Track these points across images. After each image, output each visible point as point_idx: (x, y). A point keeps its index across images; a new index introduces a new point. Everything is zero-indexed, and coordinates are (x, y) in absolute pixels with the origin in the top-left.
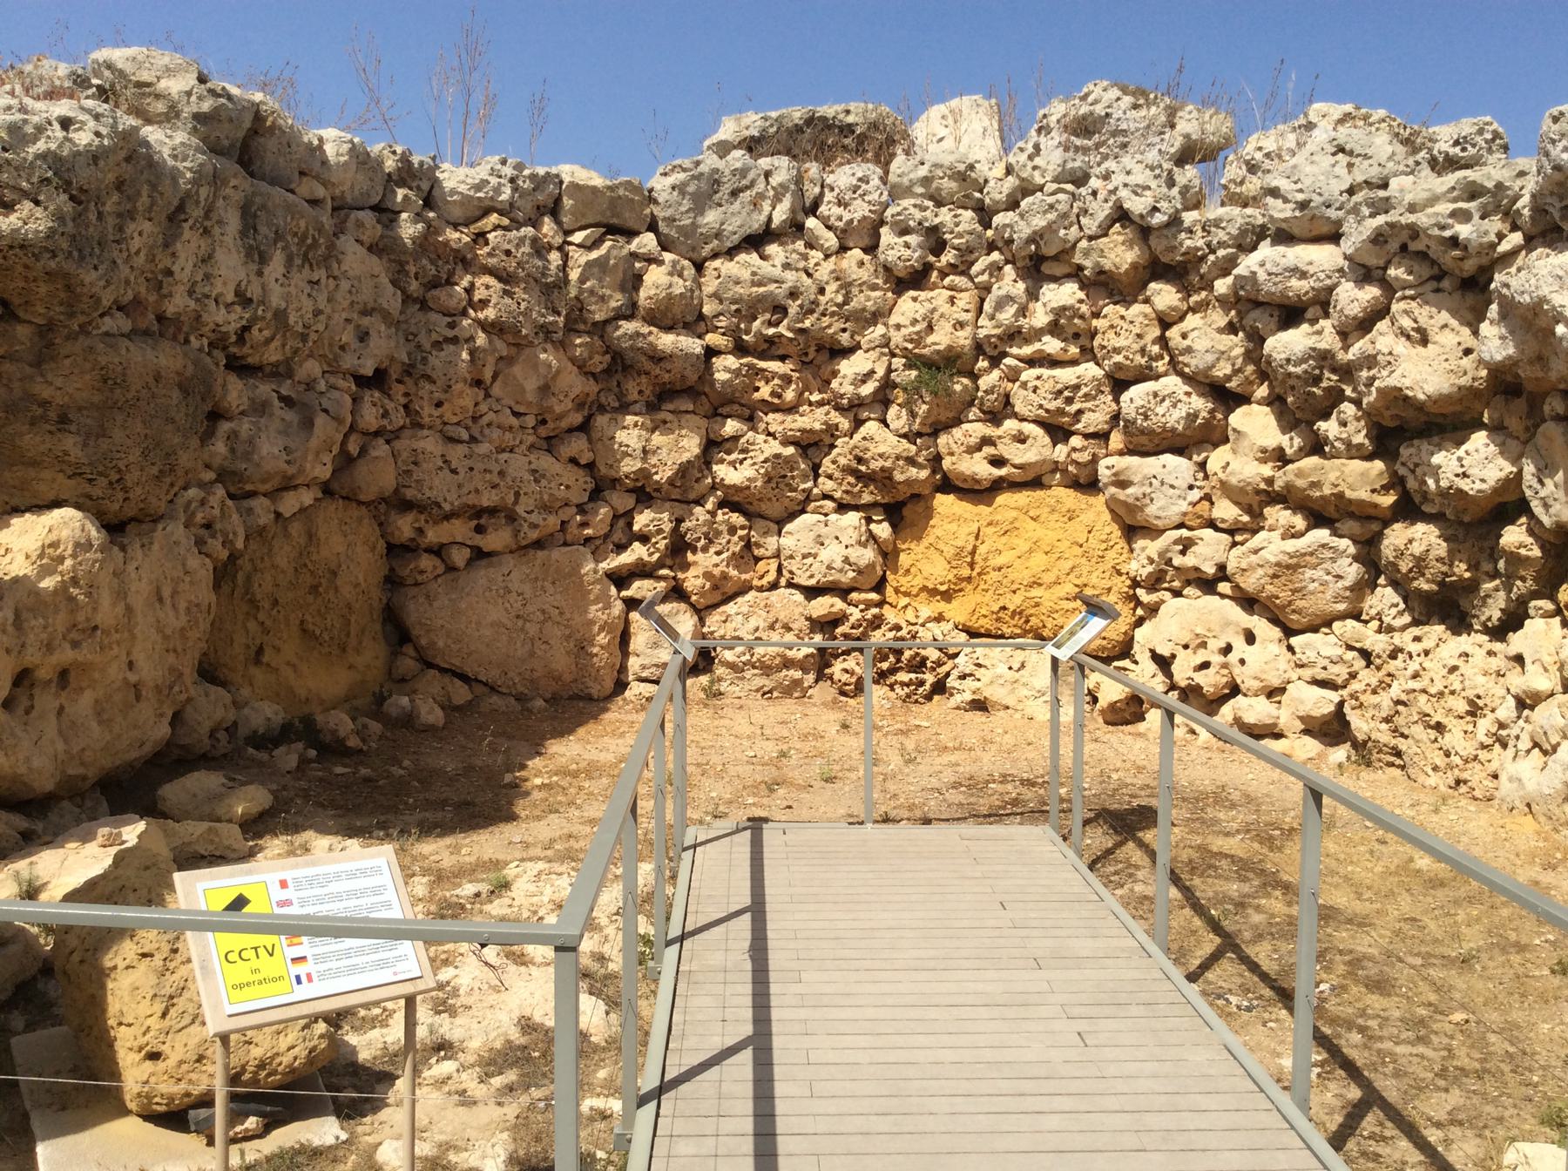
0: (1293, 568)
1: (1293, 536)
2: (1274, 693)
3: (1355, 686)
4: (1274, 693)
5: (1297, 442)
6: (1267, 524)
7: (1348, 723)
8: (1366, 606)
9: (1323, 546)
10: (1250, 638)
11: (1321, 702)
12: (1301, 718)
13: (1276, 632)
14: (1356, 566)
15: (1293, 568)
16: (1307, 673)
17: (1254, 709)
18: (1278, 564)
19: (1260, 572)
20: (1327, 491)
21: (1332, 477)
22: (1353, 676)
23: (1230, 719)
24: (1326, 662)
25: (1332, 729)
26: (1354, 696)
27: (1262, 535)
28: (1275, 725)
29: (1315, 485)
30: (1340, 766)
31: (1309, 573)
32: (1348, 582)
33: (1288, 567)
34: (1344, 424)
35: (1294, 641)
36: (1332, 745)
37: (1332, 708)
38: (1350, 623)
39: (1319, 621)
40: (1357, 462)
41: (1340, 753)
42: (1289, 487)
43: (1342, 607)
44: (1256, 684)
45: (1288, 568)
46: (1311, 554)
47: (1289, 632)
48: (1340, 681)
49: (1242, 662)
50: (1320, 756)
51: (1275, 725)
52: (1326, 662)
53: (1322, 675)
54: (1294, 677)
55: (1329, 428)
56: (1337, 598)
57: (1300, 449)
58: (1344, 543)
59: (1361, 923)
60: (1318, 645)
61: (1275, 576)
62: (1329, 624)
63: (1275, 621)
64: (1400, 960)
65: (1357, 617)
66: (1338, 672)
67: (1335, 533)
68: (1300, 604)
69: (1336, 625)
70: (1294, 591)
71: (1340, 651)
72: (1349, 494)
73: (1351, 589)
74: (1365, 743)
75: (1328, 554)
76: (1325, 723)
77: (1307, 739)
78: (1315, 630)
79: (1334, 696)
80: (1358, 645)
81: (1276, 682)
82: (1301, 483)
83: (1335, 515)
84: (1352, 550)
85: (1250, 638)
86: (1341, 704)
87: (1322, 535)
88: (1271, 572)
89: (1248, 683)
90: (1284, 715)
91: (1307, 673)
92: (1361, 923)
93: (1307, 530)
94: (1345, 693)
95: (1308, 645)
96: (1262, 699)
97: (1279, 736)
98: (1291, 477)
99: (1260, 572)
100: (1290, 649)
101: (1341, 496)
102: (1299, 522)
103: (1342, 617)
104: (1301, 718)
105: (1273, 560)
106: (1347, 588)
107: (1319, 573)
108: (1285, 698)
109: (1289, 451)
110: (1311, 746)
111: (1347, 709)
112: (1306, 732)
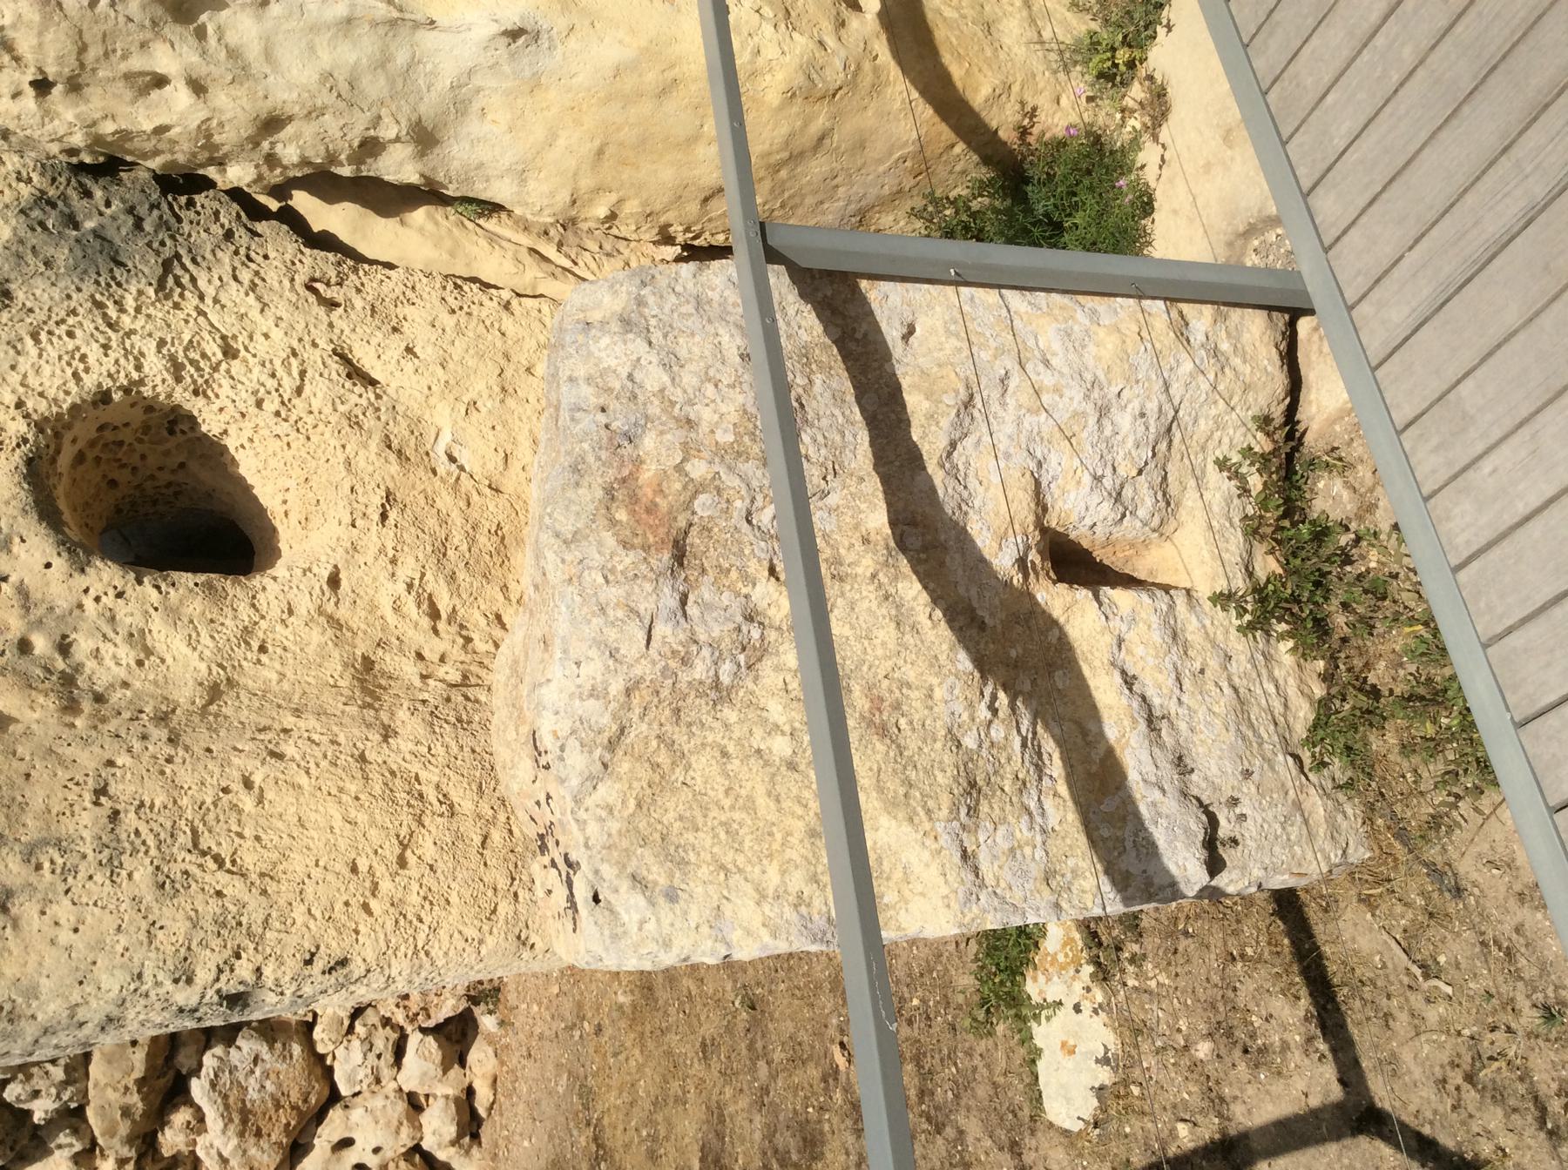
0: (245, 1114)
1: (200, 1117)
2: (415, 1104)
3: (400, 1017)
4: (415, 1104)
5: (63, 1138)
6: (185, 1150)
7: (448, 1021)
8: (294, 1019)
9: (213, 1085)
10: (347, 1143)
11: (422, 1056)
12: (445, 1072)
13: (335, 1114)
14: (240, 1042)
15: (245, 1114)
16: (386, 1073)
17: (438, 1129)
18: (241, 1134)
19: (253, 1151)
20: (135, 1099)
21: (112, 1095)
22: (386, 1022)
23: (452, 1150)
24: (371, 1057)
25: (456, 1036)
26: (413, 1019)
27: (200, 1153)
28: (457, 1101)
29: (126, 1112)
30: (502, 1023)
31: (253, 1094)
32: (263, 1049)
33: (244, 1121)
34: (36, 1094)
35: (344, 1090)
36: (477, 1027)
37: (430, 1039)
38: (318, 1034)
39: (319, 1071)
40: (92, 1068)
41: (487, 1022)
42: (130, 1141)
43: (296, 1049)
44: (405, 1131)
45: (245, 1120)
46: (225, 1097)
47: (334, 1097)
48: (396, 1036)
49: (376, 1150)
50: (491, 1040)
51: (457, 1101)
52: (371, 1057)
53: (389, 1057)
54: (393, 1085)
55: (40, 1110)
56: (286, 1056)
57: (75, 1132)
58: (209, 1061)
59: (717, 1117)
60: (348, 1067)
61: (258, 1134)
62: (322, 1057)
63: (320, 1116)
64: (765, 1090)
65: (310, 1026)
66: (383, 1040)
67: (196, 1071)
68: (295, 1096)
69: (320, 1049)
70: (278, 1106)
71: (356, 1043)
72: (138, 1073)
73: (271, 1042)
74: (470, 998)
75: (225, 1078)
76: (449, 1038)
77: (473, 1056)
78: (330, 1070)
79: (414, 1039)
80: (347, 1023)
81: (402, 1106)
82: (124, 1128)
83: (171, 1074)
84: (218, 1050)
85: (347, 1143)
86: (424, 1031)
87: (198, 1089)
88: (252, 1140)
89: (406, 1139)
90: (448, 1088)
91: (386, 1073)
92: (717, 1117)
93: (190, 1102)
94: (409, 1029)
95: (350, 1080)
96: (424, 1118)
97: (470, 1092)
98: (116, 1142)
99: (253, 1151)
100: (356, 1095)
101: (140, 1083)
102: (181, 1117)
103: (309, 1044)
104: (445, 1072)
105: (235, 1141)
106: (271, 1048)
107: (252, 1084)
108: (421, 1091)
109: (78, 1147)
110: (480, 1056)
111: (431, 1023)
112: (462, 1062)
